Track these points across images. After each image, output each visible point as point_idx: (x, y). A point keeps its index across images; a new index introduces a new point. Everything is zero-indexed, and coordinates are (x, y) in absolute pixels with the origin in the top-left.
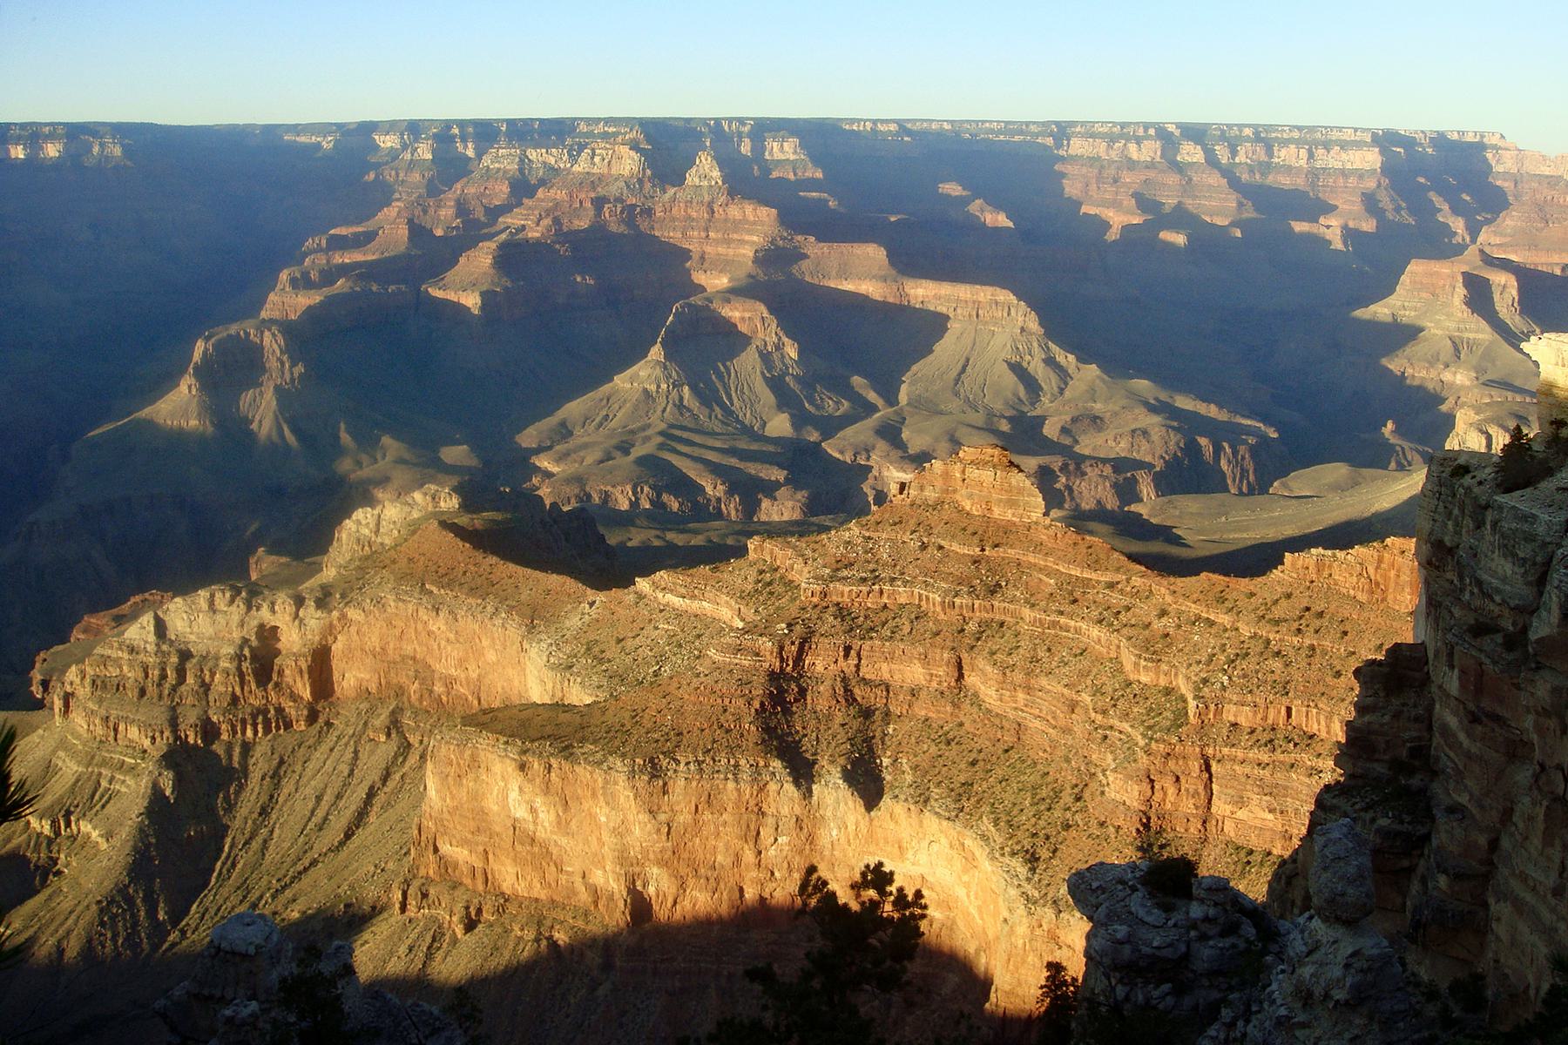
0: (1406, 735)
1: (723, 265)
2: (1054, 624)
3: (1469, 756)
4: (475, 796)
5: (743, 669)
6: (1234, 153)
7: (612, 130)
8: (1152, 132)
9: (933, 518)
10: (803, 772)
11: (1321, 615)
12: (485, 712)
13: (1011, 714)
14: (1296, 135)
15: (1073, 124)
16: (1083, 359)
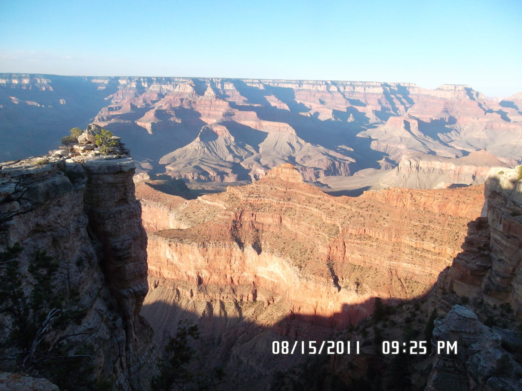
0: (483, 241)
1: (215, 117)
2: (305, 208)
3: (506, 247)
4: (157, 253)
5: (227, 220)
6: (345, 89)
7: (184, 80)
8: (324, 83)
9: (274, 181)
10: (241, 245)
11: (373, 206)
12: (160, 231)
13: (294, 231)
14: (361, 84)
15: (304, 81)
16: (307, 141)
